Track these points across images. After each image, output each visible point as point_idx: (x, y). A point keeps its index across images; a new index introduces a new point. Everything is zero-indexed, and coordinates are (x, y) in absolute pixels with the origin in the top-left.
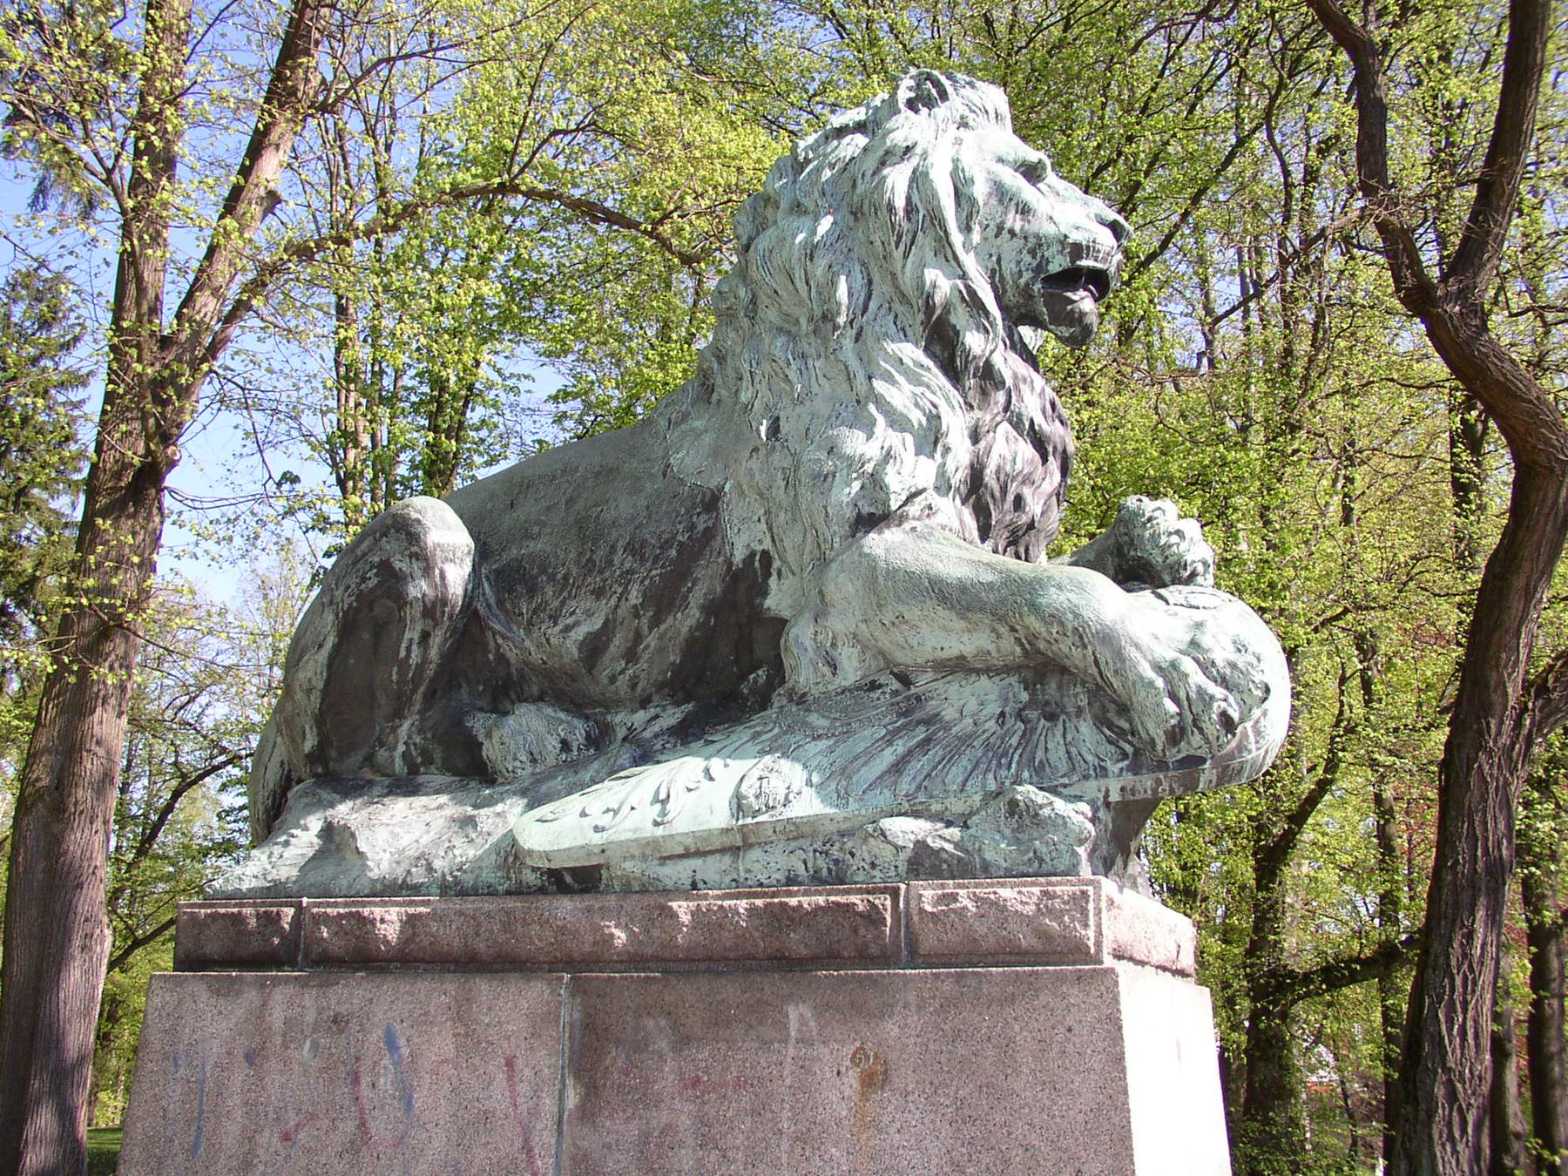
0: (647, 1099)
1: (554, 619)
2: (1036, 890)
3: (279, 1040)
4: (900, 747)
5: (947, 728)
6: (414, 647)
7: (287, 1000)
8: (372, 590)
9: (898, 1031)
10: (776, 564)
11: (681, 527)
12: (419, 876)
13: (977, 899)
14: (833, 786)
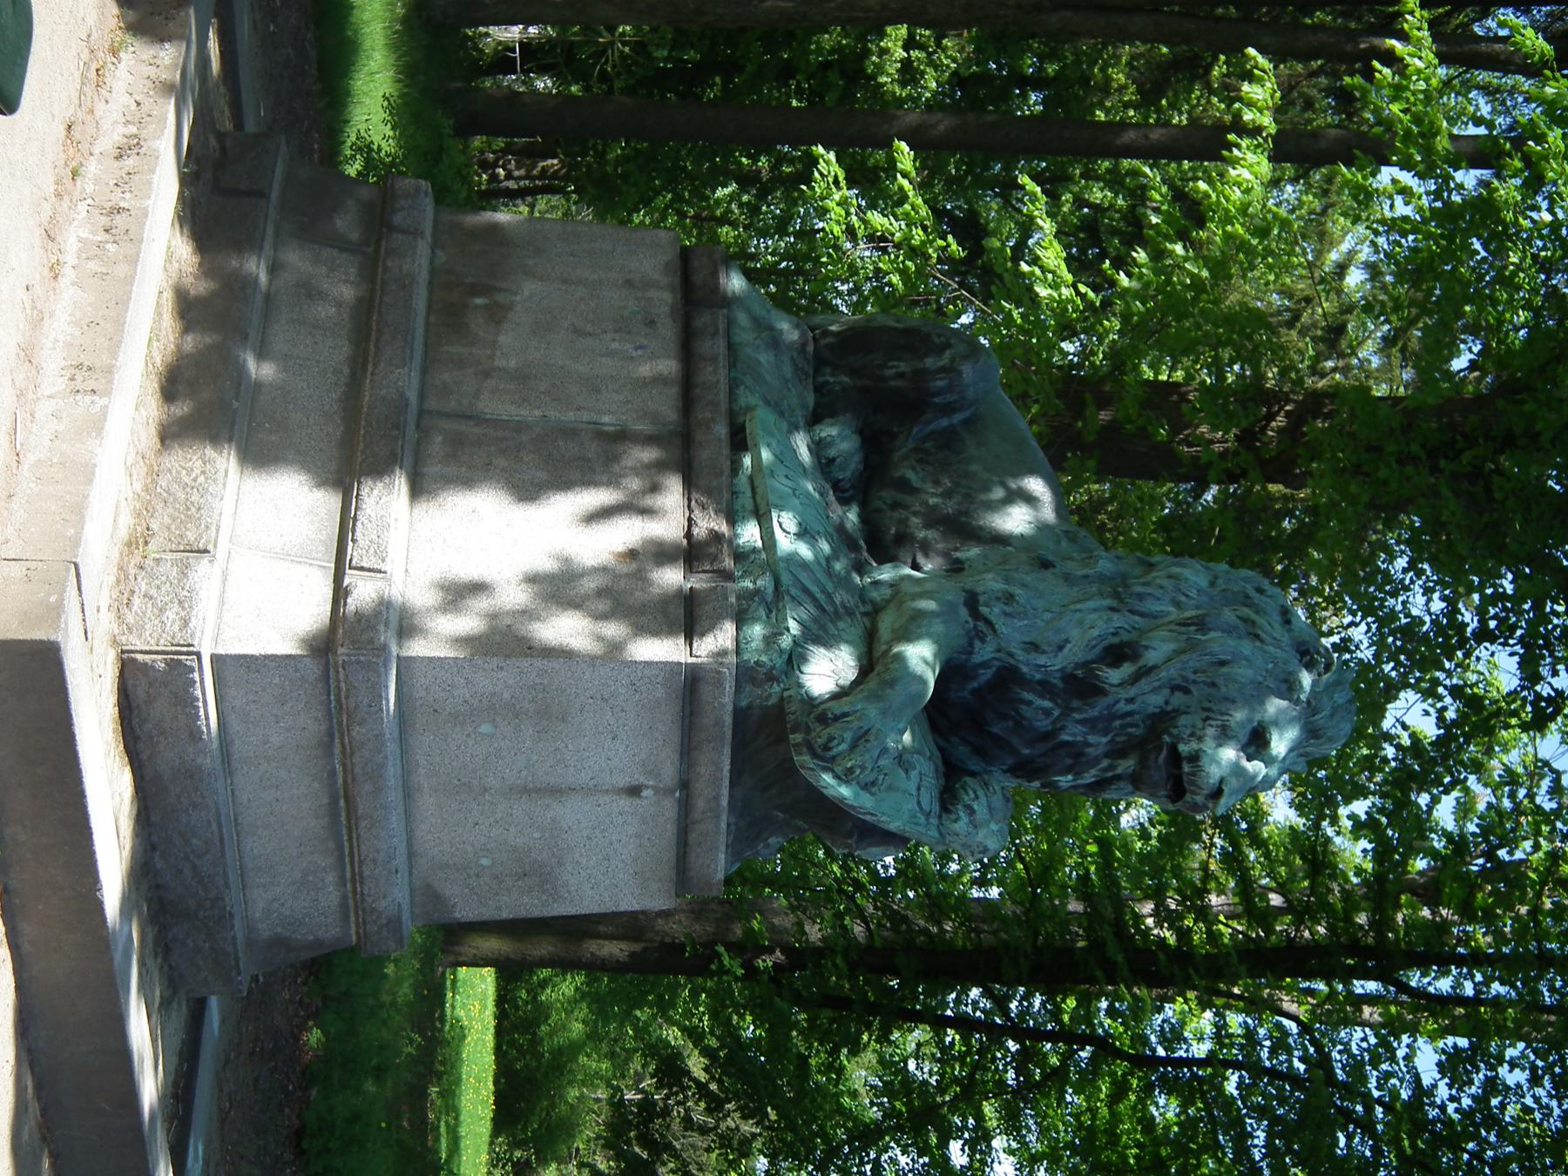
4: (818, 595)
5: (831, 621)
7: (664, 299)
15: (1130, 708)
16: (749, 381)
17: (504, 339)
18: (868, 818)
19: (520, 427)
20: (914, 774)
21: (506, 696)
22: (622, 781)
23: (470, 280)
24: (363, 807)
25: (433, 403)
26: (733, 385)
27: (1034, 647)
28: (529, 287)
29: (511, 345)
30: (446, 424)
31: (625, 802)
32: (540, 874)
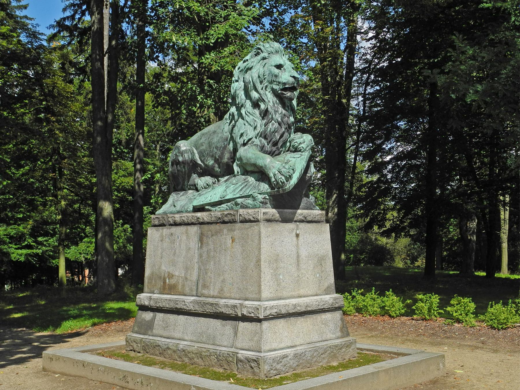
0: (208, 244)
1: (207, 161)
4: (242, 187)
9: (237, 233)
15: (271, 102)
16: (186, 207)
17: (177, 274)
18: (303, 171)
19: (200, 269)
20: (290, 159)
21: (272, 271)
22: (295, 239)
23: (162, 283)
24: (303, 309)
25: (194, 293)
26: (187, 212)
27: (255, 128)
28: (163, 268)
29: (178, 272)
30: (200, 289)
31: (301, 238)
32: (321, 259)
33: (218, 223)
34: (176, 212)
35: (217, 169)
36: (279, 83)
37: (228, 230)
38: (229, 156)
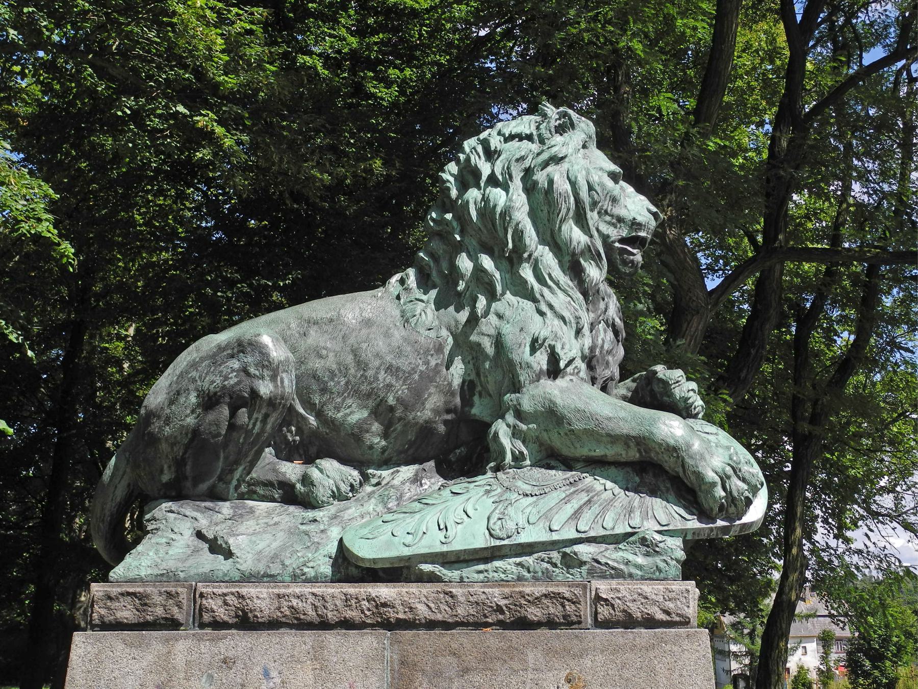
2: (661, 587)
3: (182, 675)
4: (575, 504)
6: (258, 423)
7: (185, 647)
8: (233, 386)
10: (479, 388)
11: (420, 362)
12: (275, 569)
13: (631, 592)
14: (541, 525)
16: (292, 563)
33: (487, 625)
34: (237, 576)
35: (375, 439)
36: (620, 220)
37: (550, 652)
38: (440, 404)
